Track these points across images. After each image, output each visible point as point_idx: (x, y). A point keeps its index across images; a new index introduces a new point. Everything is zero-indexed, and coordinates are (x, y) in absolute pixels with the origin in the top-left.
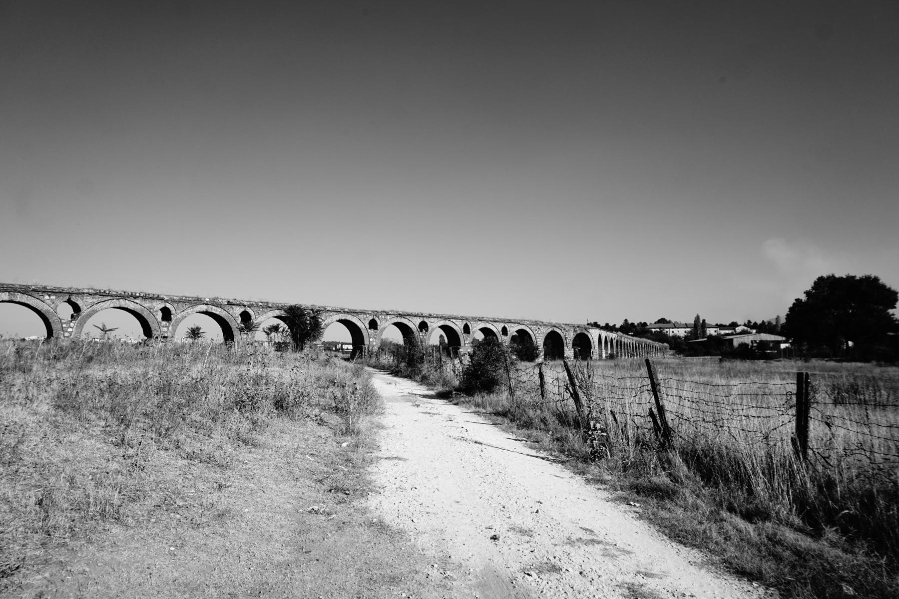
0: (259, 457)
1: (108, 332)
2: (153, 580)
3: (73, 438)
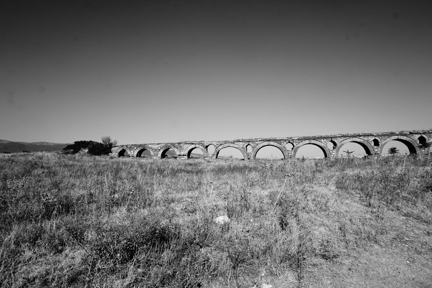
1: (350, 154)
2: (401, 276)
3: (347, 201)
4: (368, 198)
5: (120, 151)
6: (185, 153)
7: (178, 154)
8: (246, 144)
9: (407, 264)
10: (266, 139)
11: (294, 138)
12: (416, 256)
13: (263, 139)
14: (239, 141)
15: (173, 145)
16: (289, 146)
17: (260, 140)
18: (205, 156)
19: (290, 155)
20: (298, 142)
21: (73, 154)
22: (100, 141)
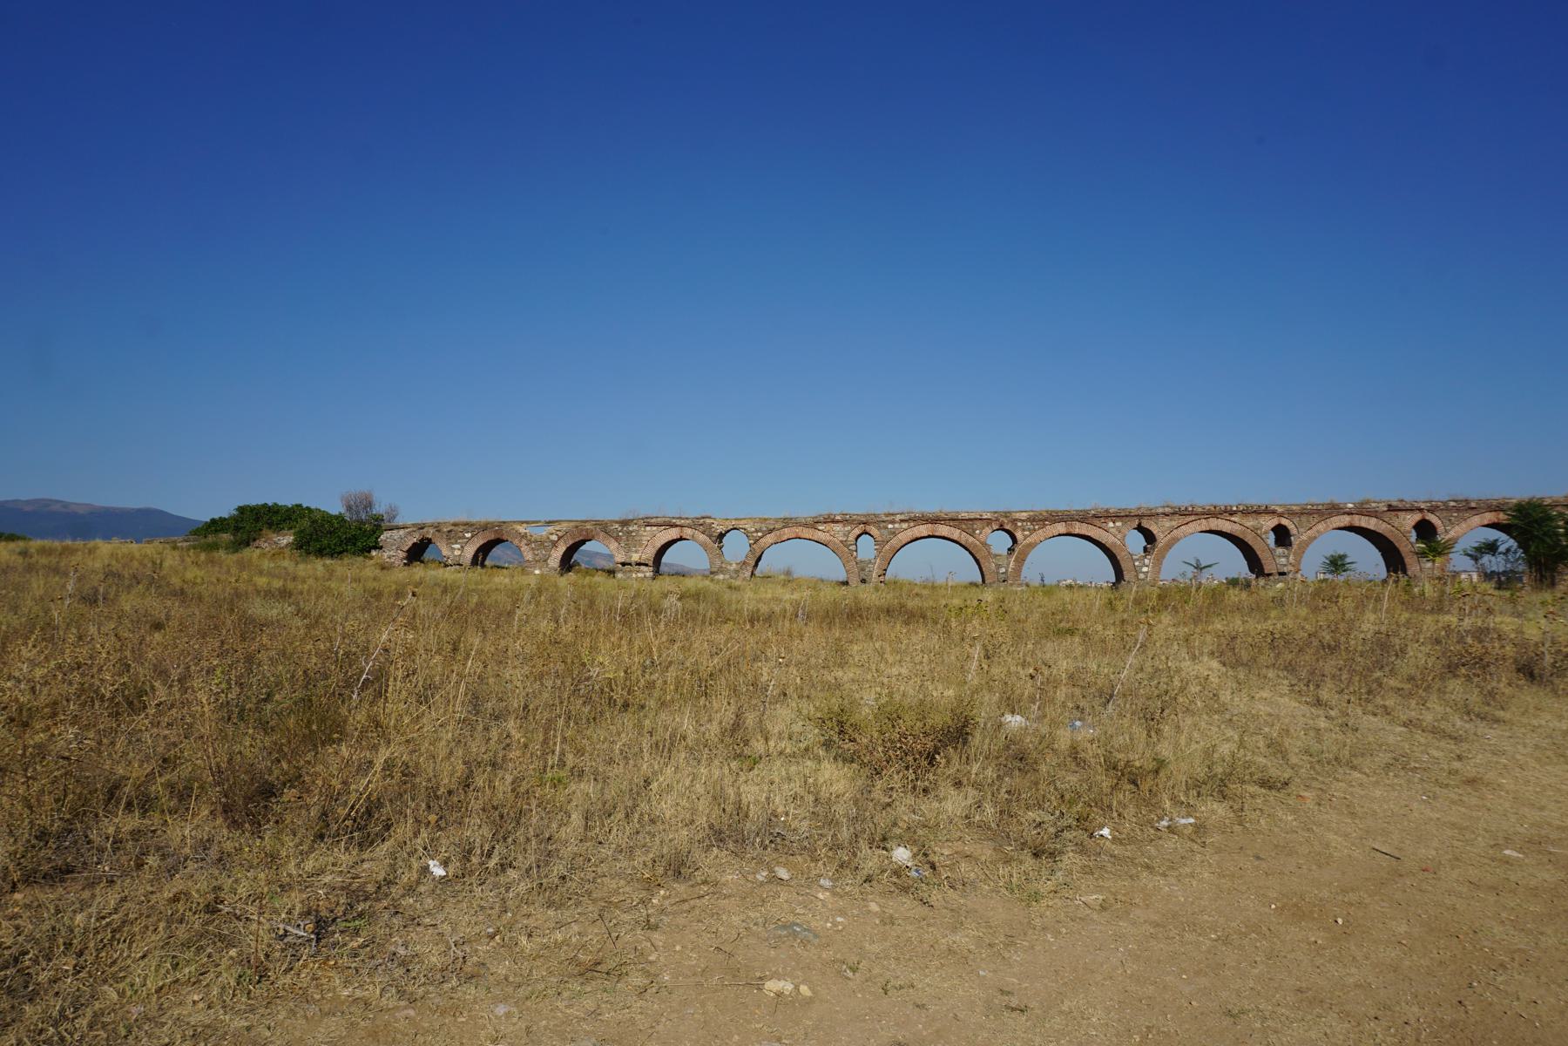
0: (1508, 734)
1: (1204, 571)
3: (1265, 694)
4: (1312, 688)
5: (414, 544)
6: (644, 557)
7: (620, 558)
8: (857, 531)
9: (1424, 801)
10: (923, 516)
11: (1017, 516)
12: (1437, 789)
13: (915, 517)
14: (833, 521)
15: (604, 527)
16: (1000, 542)
17: (903, 517)
18: (715, 570)
19: (1003, 570)
20: (1029, 530)
21: (236, 551)
22: (335, 508)
